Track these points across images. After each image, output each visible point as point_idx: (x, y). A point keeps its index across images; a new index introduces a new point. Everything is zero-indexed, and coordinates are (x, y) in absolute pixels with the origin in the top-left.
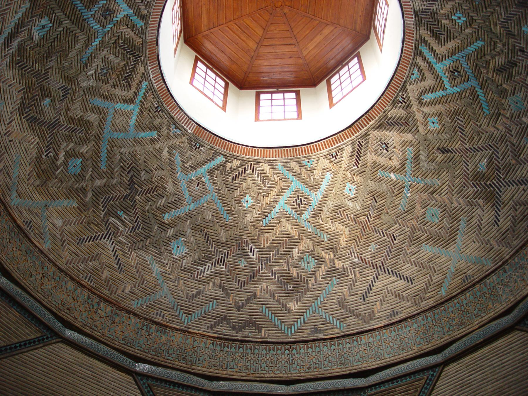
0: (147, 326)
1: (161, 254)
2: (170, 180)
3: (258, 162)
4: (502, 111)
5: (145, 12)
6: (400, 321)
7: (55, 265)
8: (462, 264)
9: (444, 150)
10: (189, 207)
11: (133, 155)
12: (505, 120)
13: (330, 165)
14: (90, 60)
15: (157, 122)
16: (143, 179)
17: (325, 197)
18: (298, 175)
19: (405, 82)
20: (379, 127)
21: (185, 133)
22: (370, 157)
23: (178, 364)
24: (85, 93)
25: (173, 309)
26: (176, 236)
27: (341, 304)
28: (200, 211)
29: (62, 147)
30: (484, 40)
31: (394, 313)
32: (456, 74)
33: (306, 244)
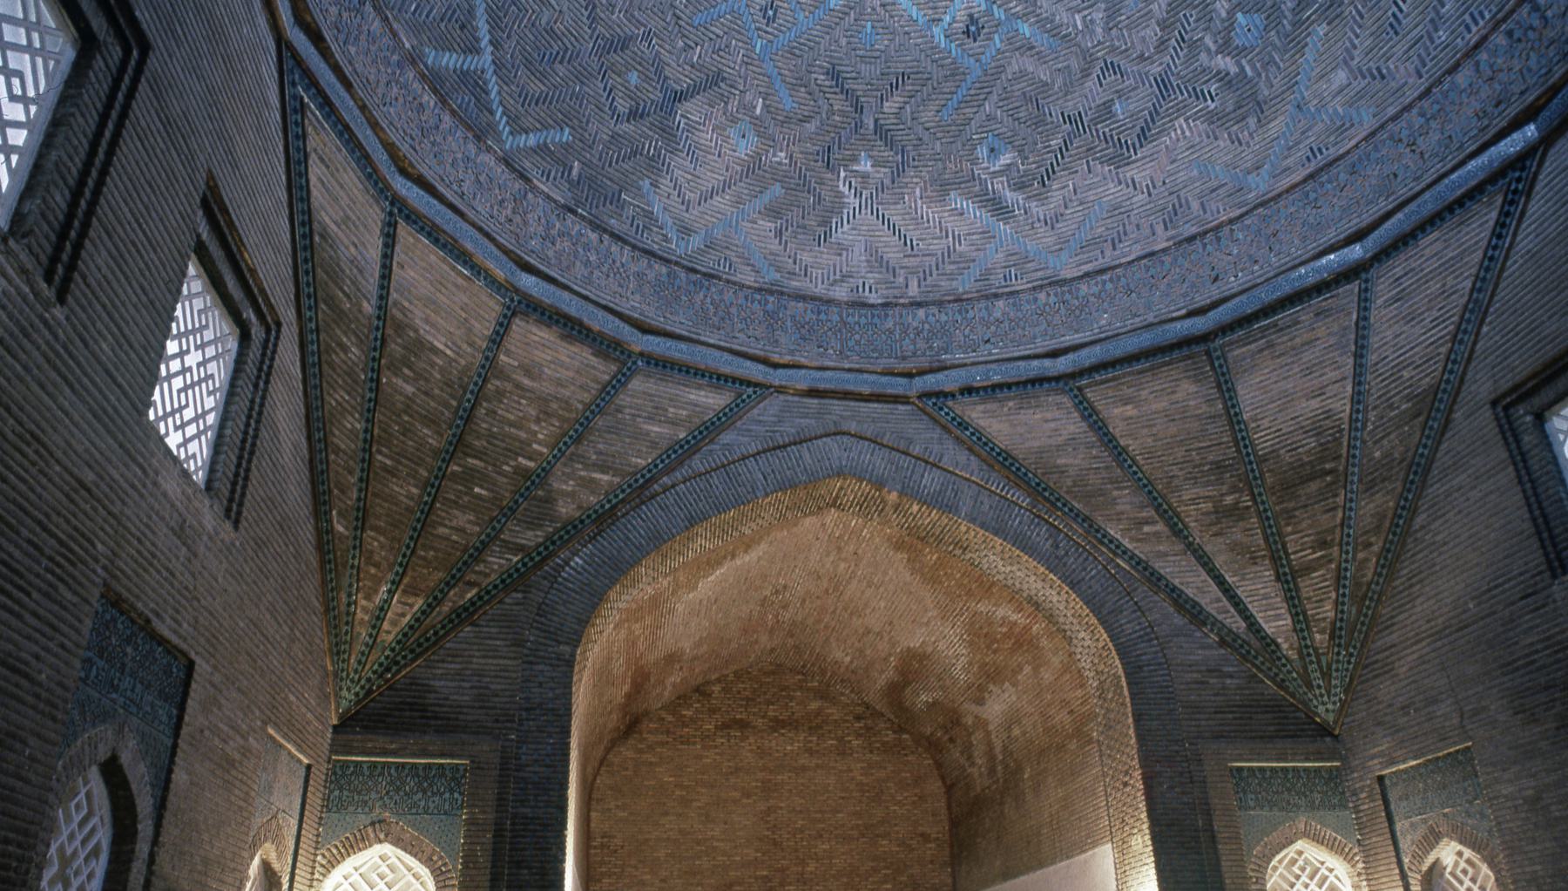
7: (1408, 108)
14: (1054, 31)
24: (1116, 26)
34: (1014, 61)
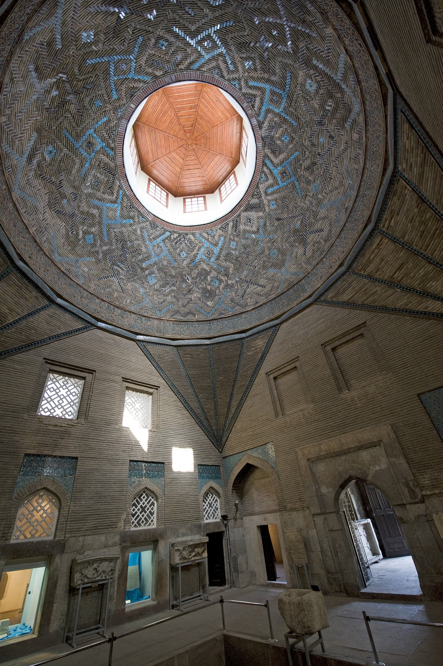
0: (140, 318)
1: (143, 283)
2: (143, 246)
3: (187, 234)
4: (308, 193)
5: (113, 145)
6: (260, 306)
7: (87, 291)
8: (288, 276)
9: (278, 219)
10: (154, 259)
11: (121, 233)
12: (309, 198)
13: (223, 233)
15: (132, 214)
16: (129, 245)
17: (221, 249)
18: (208, 240)
19: (258, 183)
20: (246, 210)
21: (147, 220)
22: (242, 227)
23: (157, 334)
25: (152, 309)
26: (150, 274)
27: (232, 300)
28: (161, 261)
29: (80, 229)
30: (299, 151)
31: (257, 303)
32: (284, 174)
33: (214, 274)
34: (78, 160)
